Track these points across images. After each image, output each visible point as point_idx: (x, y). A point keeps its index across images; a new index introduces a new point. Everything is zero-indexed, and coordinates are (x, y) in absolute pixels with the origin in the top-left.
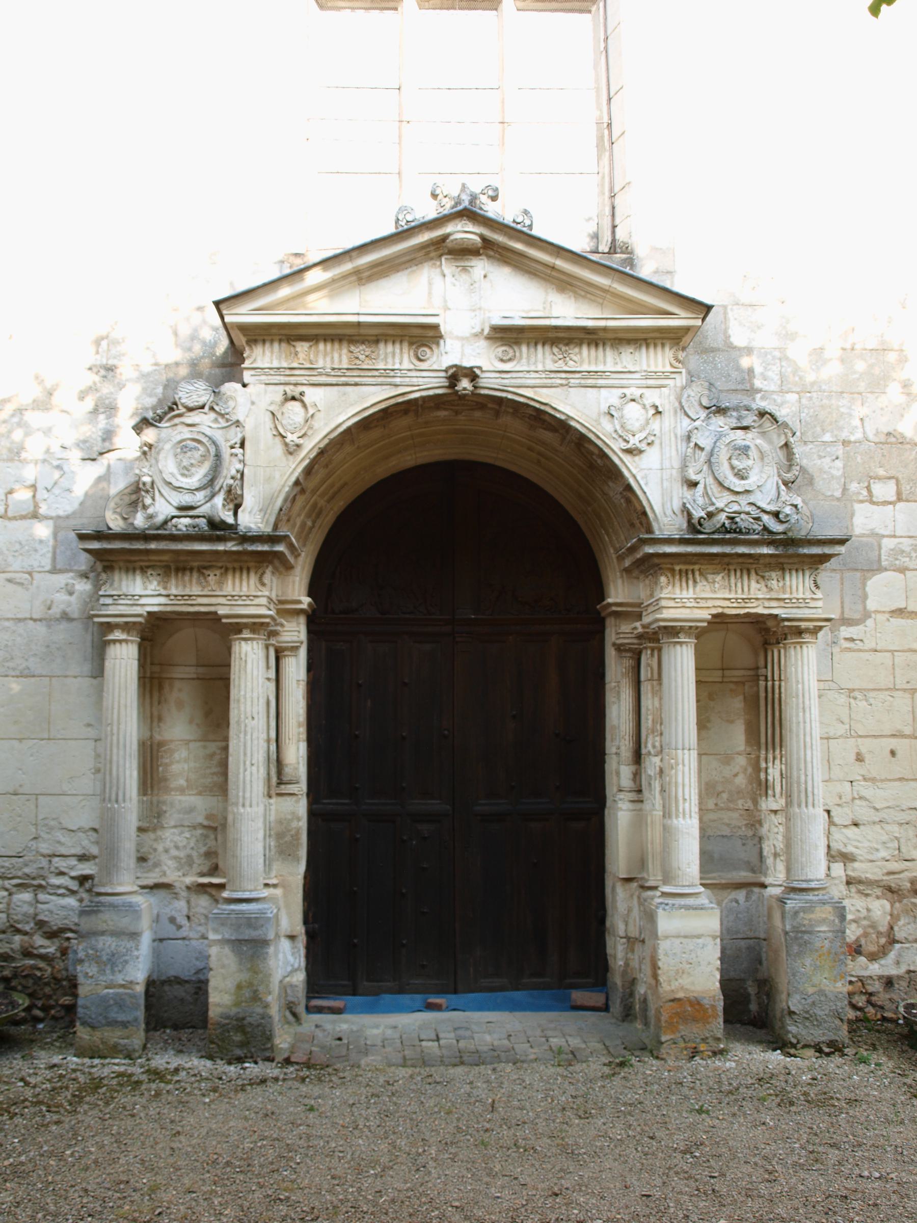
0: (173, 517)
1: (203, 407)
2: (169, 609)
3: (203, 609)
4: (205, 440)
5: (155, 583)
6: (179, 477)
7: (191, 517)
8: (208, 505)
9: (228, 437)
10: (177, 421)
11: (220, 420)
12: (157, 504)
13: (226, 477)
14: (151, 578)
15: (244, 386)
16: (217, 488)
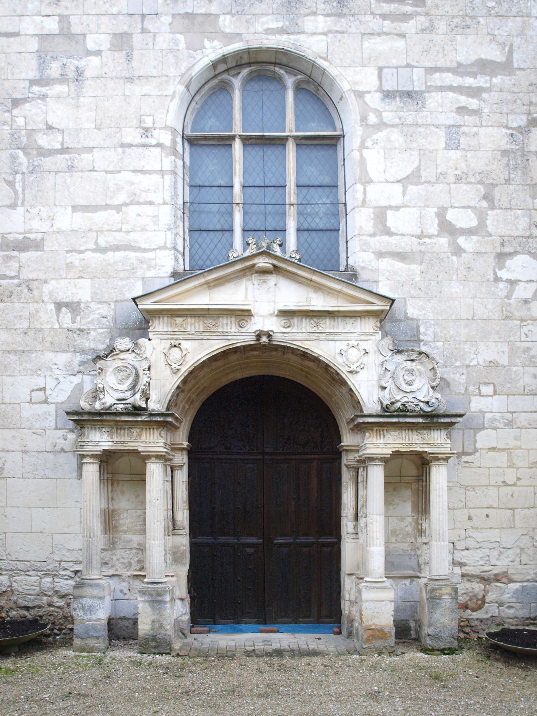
0: (114, 404)
1: (128, 350)
2: (114, 448)
3: (131, 448)
4: (130, 367)
5: (107, 436)
6: (117, 385)
7: (123, 404)
8: (132, 398)
9: (142, 365)
10: (115, 357)
11: (137, 357)
12: (106, 397)
13: (141, 385)
14: (104, 433)
15: (150, 340)
16: (137, 391)
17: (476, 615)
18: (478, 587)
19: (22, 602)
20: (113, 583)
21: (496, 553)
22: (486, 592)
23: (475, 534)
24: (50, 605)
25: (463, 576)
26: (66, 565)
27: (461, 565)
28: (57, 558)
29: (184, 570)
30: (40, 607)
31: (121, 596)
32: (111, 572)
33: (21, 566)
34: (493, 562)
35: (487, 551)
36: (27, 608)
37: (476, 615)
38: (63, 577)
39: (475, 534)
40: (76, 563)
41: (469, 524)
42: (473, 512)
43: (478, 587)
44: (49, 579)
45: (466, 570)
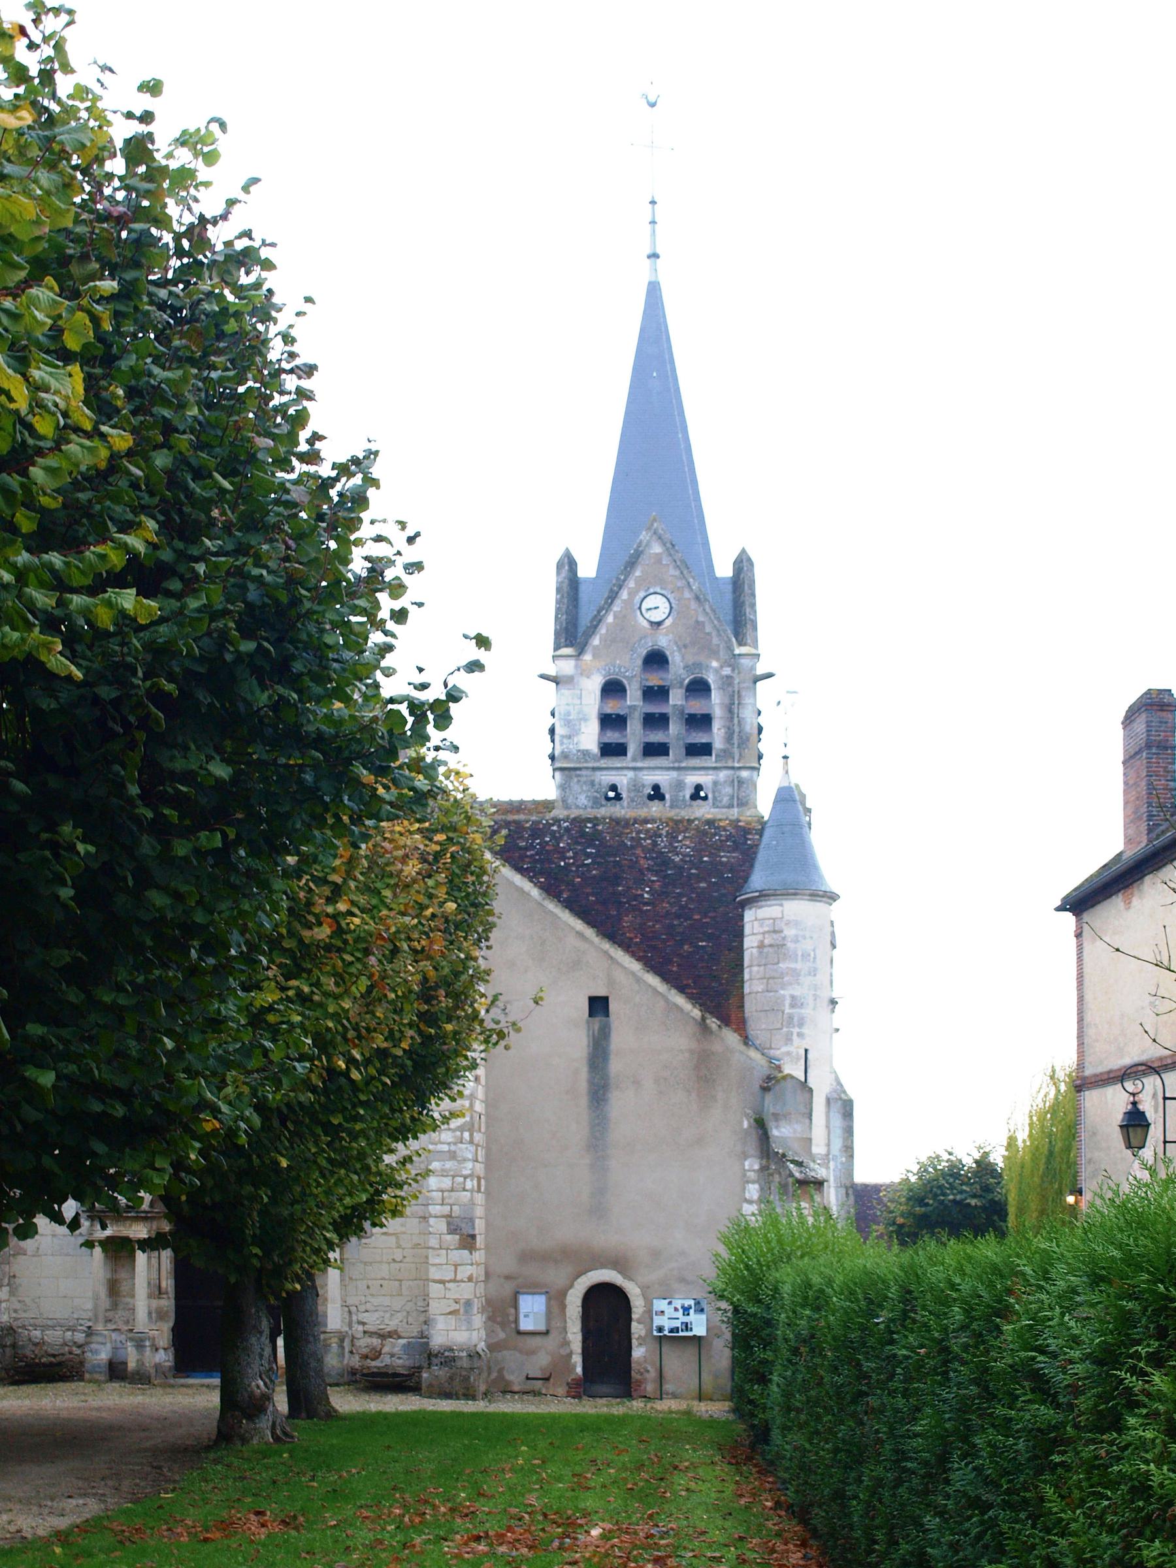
17: (374, 1363)
18: (376, 1341)
19: (50, 1351)
20: (114, 1335)
21: (388, 1315)
22: (383, 1345)
23: (372, 1300)
24: (70, 1353)
25: (365, 1332)
26: (81, 1322)
27: (364, 1324)
28: (76, 1316)
29: (167, 1326)
30: (63, 1354)
31: (119, 1345)
32: (114, 1327)
33: (50, 1323)
34: (387, 1322)
35: (382, 1314)
36: (54, 1356)
37: (374, 1363)
38: (79, 1331)
39: (372, 1300)
40: (89, 1320)
41: (367, 1292)
42: (370, 1283)
43: (376, 1341)
44: (70, 1333)
45: (367, 1328)
